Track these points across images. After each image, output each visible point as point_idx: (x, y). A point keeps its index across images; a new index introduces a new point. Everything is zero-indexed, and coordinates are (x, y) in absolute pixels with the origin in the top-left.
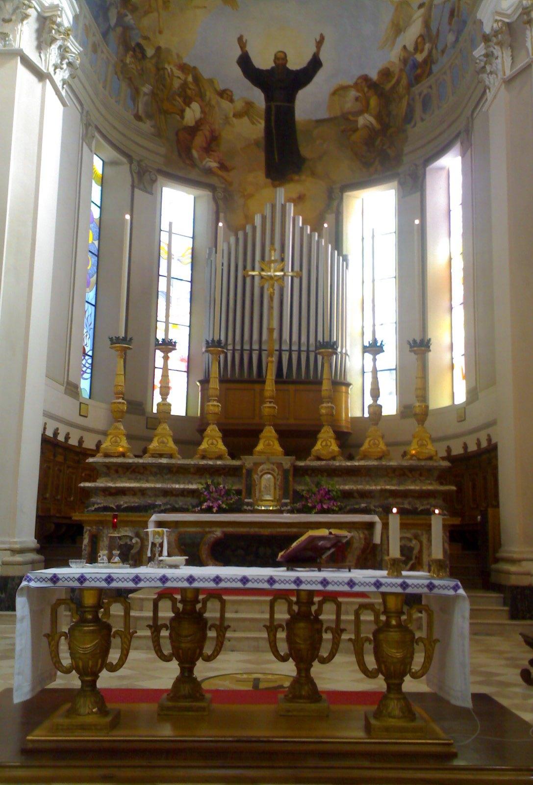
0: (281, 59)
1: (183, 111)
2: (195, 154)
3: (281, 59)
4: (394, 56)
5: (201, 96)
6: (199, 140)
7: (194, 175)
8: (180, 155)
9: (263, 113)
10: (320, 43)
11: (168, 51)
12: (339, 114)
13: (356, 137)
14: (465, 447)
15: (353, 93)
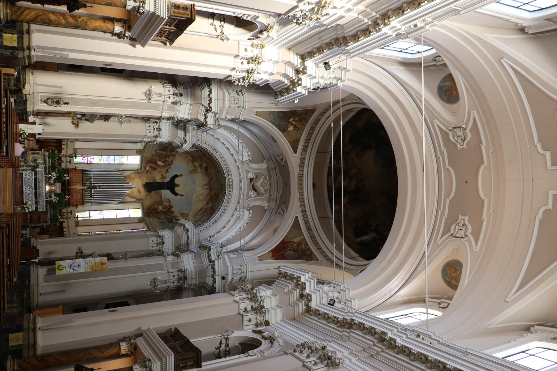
0: (178, 185)
1: (161, 161)
3: (178, 185)
4: (176, 214)
5: (166, 165)
6: (153, 165)
7: (144, 164)
8: (148, 161)
10: (182, 195)
12: (163, 201)
13: (156, 206)
14: (65, 232)
15: (168, 204)
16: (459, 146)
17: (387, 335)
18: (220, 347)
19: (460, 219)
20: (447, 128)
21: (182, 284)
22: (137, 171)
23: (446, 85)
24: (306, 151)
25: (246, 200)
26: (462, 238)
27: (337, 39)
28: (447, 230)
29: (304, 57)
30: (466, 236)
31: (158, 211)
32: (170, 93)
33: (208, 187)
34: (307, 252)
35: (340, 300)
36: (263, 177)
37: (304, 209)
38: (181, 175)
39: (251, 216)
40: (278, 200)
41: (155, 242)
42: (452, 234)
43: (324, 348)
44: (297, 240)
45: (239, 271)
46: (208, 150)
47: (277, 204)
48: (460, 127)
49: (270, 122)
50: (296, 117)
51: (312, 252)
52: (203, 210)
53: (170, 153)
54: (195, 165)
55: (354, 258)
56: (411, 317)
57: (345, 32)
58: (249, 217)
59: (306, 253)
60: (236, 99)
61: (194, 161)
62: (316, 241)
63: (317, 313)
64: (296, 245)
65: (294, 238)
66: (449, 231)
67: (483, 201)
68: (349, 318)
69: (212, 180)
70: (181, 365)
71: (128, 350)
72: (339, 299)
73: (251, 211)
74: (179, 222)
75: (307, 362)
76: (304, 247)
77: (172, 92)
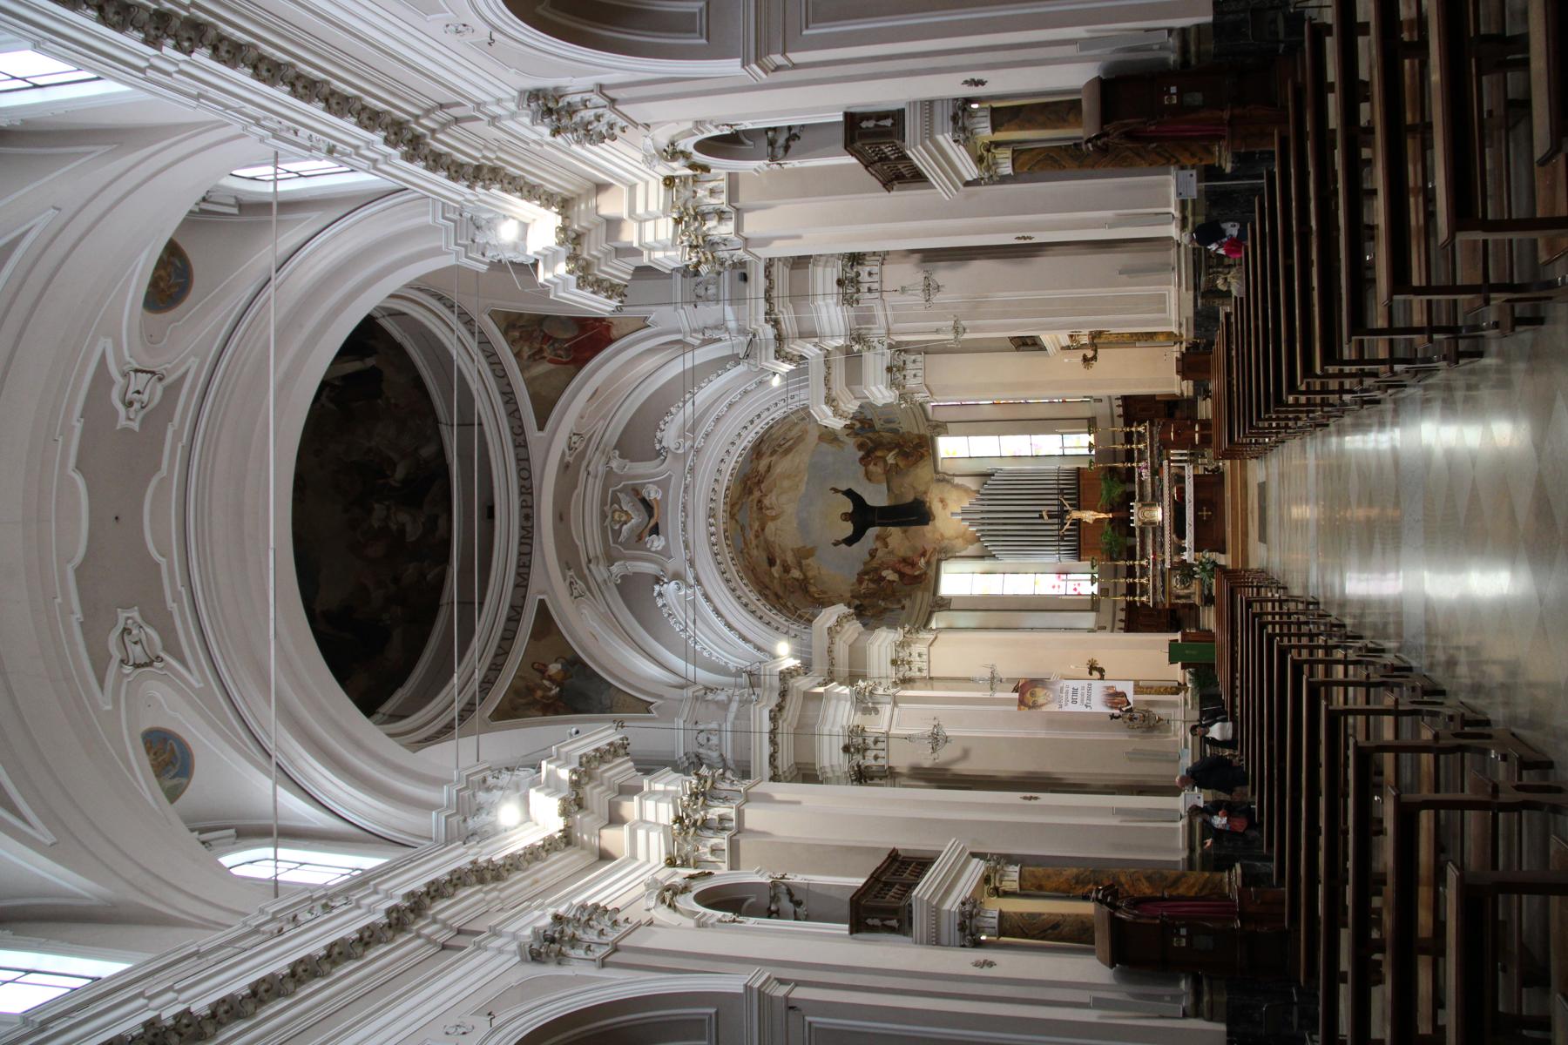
2: (917, 573)
4: (851, 442)
5: (877, 570)
6: (908, 570)
7: (932, 573)
9: (883, 528)
10: (836, 490)
11: (852, 591)
12: (884, 477)
13: (901, 464)
15: (871, 467)
16: (139, 620)
17: (402, 153)
18: (788, 140)
19: (138, 419)
20: (168, 667)
21: (848, 270)
22: (950, 555)
23: (174, 777)
24: (512, 607)
25: (670, 476)
26: (137, 371)
27: (498, 878)
28: (172, 391)
29: (564, 840)
30: (125, 375)
31: (897, 450)
32: (875, 752)
33: (768, 512)
34: (517, 334)
35: (470, 223)
36: (622, 539)
37: (520, 449)
38: (836, 544)
39: (659, 434)
40: (583, 475)
41: (910, 373)
42: (160, 379)
43: (556, 132)
44: (542, 368)
45: (702, 292)
46: (770, 610)
47: (585, 463)
48: (137, 666)
49: (610, 685)
50: (543, 697)
51: (505, 334)
52: (781, 450)
53: (866, 602)
54: (801, 570)
55: (390, 315)
56: (289, 172)
57: (481, 895)
58: (662, 430)
59: (521, 332)
60: (704, 742)
61: (803, 580)
62: (491, 364)
63: (548, 199)
64: (545, 354)
65: (547, 375)
66: (166, 390)
67: (78, 467)
68: (478, 189)
69: (757, 531)
70: (888, 122)
71: (997, 156)
72: (474, 224)
73: (658, 447)
74: (848, 422)
75: (605, 107)
76: (526, 349)
77: (870, 754)
